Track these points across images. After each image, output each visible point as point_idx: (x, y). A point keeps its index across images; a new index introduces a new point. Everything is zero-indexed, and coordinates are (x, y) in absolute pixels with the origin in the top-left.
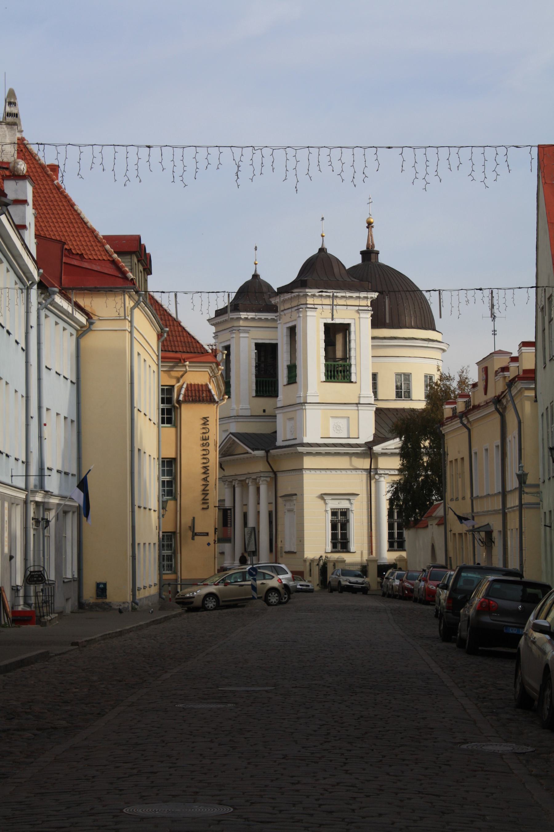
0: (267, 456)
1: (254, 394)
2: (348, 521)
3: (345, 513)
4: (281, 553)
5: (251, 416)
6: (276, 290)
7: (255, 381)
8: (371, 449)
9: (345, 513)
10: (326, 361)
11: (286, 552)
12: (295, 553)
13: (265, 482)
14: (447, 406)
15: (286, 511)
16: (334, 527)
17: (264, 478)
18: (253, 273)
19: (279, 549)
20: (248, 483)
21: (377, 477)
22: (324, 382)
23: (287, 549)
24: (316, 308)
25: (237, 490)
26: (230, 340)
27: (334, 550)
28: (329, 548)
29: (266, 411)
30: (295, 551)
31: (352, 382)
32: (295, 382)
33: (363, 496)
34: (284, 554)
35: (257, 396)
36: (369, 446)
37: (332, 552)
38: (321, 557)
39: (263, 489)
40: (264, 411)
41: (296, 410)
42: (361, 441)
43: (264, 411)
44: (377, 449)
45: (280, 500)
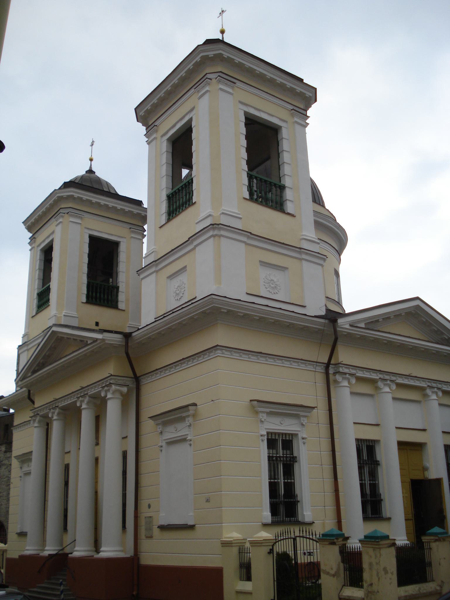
3: (288, 442)
4: (149, 529)
7: (86, 282)
9: (288, 442)
11: (162, 528)
12: (192, 527)
13: (118, 395)
15: (164, 444)
17: (118, 388)
18: (88, 169)
19: (142, 522)
21: (338, 377)
23: (163, 522)
24: (235, 83)
25: (56, 427)
27: (276, 519)
29: (100, 324)
30: (191, 523)
33: (321, 413)
34: (156, 531)
39: (113, 408)
40: (97, 324)
41: (194, 249)
43: (97, 324)
45: (148, 426)
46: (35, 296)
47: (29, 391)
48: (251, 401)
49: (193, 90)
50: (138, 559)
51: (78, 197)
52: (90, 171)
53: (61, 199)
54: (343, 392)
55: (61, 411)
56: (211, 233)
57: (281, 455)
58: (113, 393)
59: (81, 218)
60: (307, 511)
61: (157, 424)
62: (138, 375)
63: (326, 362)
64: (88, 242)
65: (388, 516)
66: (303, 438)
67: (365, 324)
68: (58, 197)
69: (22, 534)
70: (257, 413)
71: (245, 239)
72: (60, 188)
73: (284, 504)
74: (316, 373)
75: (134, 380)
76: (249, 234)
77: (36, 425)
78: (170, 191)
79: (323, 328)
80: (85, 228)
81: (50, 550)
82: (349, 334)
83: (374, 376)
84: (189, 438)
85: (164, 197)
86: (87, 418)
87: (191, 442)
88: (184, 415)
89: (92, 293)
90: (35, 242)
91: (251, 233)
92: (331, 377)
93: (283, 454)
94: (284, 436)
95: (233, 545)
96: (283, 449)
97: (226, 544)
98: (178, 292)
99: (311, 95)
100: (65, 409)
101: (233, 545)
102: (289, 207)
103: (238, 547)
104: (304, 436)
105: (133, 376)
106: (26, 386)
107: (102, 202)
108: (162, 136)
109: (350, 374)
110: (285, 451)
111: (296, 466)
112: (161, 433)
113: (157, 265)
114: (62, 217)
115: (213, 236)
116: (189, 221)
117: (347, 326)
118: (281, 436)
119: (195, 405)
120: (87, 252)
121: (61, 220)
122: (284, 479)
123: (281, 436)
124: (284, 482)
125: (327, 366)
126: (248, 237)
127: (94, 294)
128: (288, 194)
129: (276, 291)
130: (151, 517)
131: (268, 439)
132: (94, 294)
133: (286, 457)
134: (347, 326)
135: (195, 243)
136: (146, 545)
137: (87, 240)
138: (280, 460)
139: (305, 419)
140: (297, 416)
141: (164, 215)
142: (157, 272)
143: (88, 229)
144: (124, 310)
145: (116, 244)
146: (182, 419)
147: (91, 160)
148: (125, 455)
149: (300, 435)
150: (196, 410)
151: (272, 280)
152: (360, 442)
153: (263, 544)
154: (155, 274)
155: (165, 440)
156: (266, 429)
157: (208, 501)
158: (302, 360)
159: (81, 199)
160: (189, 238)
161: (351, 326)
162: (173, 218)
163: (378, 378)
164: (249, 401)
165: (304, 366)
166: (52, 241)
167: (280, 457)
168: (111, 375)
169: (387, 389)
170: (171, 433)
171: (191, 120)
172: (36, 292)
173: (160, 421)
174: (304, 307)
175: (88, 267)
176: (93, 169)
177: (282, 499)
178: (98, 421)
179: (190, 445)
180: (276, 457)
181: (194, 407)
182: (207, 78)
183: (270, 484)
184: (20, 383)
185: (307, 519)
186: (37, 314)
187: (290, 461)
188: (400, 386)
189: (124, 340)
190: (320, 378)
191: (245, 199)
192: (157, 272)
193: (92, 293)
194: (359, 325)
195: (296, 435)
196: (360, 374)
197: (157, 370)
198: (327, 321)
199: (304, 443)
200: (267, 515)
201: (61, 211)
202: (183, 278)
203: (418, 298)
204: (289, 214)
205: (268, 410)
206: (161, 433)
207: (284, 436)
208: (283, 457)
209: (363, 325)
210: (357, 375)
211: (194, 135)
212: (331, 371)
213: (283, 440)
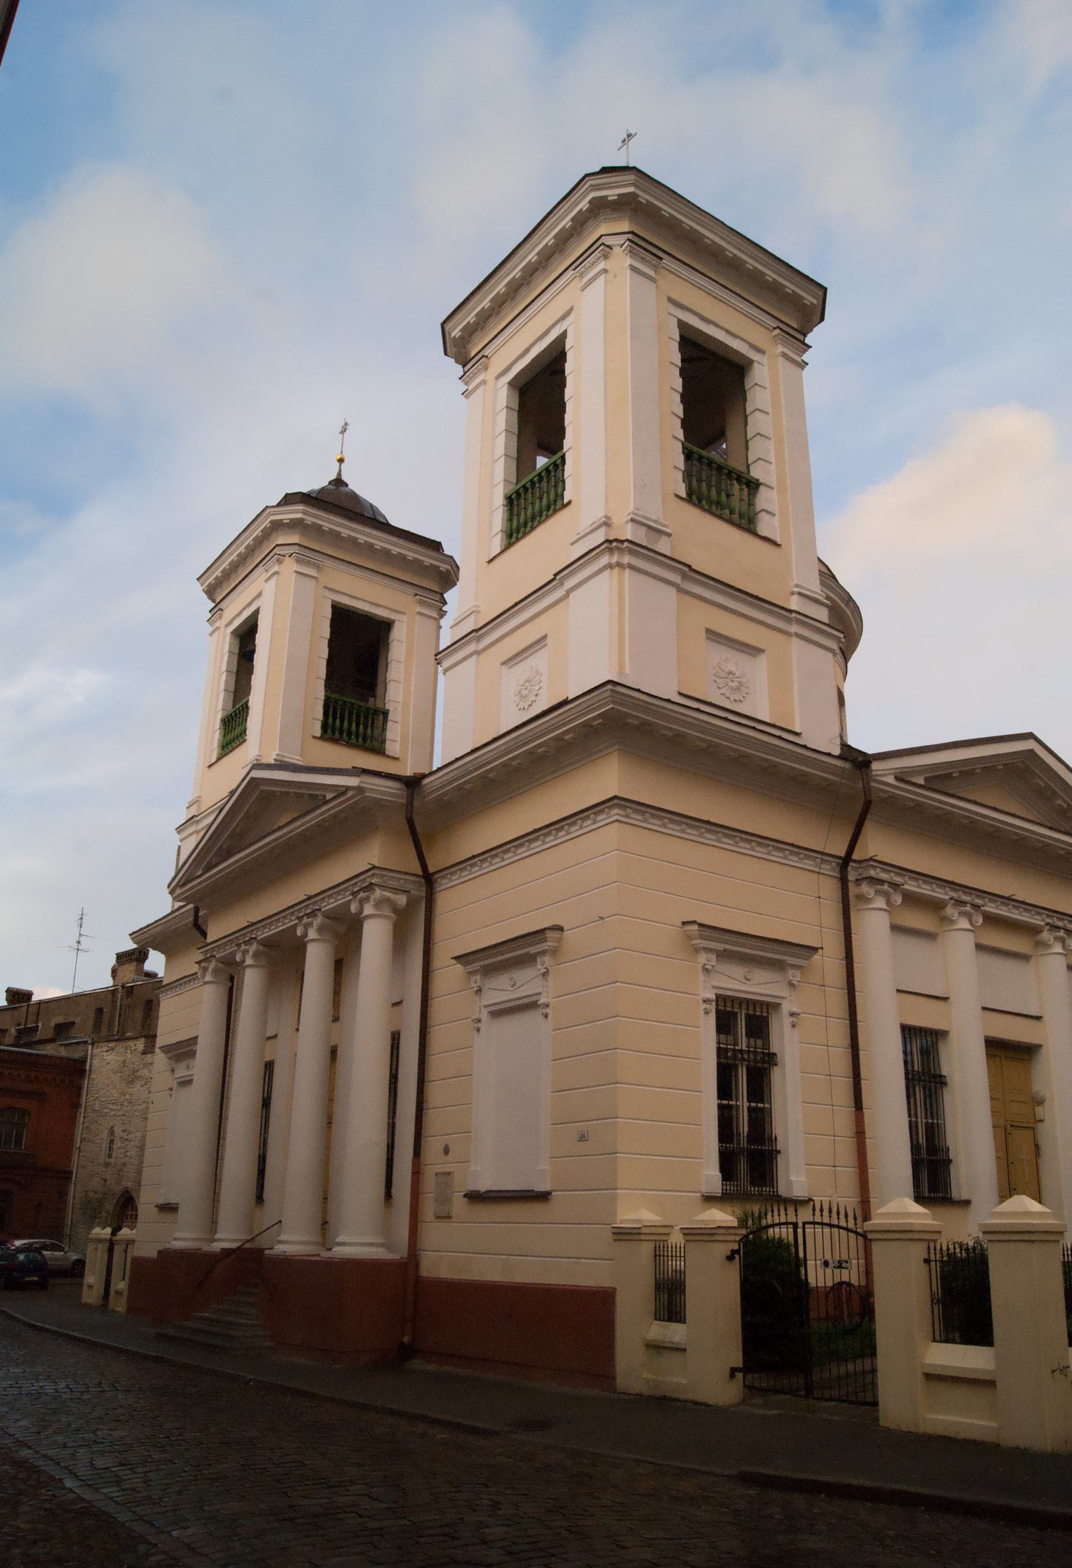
0: (410, 804)
1: (318, 734)
2: (771, 1059)
4: (444, 1199)
11: (475, 1197)
12: (543, 1197)
15: (484, 1015)
17: (387, 894)
18: (334, 477)
19: (429, 1182)
21: (866, 889)
22: (681, 498)
24: (661, 259)
25: (252, 980)
27: (731, 1187)
33: (830, 962)
34: (459, 1205)
35: (322, 738)
39: (376, 935)
45: (449, 976)
46: (218, 724)
47: (197, 910)
48: (684, 923)
49: (570, 273)
50: (417, 1265)
51: (313, 523)
52: (339, 482)
53: (277, 526)
54: (874, 924)
55: (261, 948)
56: (605, 560)
57: (744, 1048)
58: (378, 905)
59: (318, 568)
60: (795, 1176)
61: (471, 973)
62: (431, 870)
63: (842, 854)
64: (330, 616)
65: (965, 1196)
66: (792, 1015)
67: (926, 779)
68: (271, 522)
70: (697, 950)
71: (676, 578)
72: (279, 505)
73: (748, 1156)
74: (821, 877)
75: (423, 881)
76: (687, 569)
77: (208, 978)
78: (512, 488)
79: (839, 780)
80: (325, 587)
81: (227, 1238)
82: (893, 796)
83: (940, 894)
84: (543, 1000)
85: (499, 500)
86: (317, 958)
87: (548, 1011)
88: (532, 950)
89: (334, 719)
90: (220, 617)
91: (689, 567)
92: (853, 889)
94: (751, 1008)
95: (643, 1237)
97: (625, 1235)
98: (525, 692)
99: (815, 302)
100: (269, 944)
101: (643, 1237)
102: (766, 525)
103: (652, 1244)
104: (795, 1009)
106: (188, 900)
107: (362, 538)
108: (497, 378)
110: (752, 1041)
111: (776, 1074)
112: (479, 991)
113: (479, 639)
114: (279, 562)
115: (610, 566)
116: (553, 541)
117: (891, 780)
118: (744, 1007)
119: (561, 929)
120: (328, 635)
121: (276, 568)
123: (744, 1007)
125: (846, 861)
126: (684, 577)
127: (338, 722)
128: (765, 499)
130: (449, 1173)
131: (718, 1011)
132: (338, 722)
133: (755, 1053)
134: (891, 780)
135: (569, 584)
136: (433, 1234)
137: (328, 613)
138: (743, 1059)
139: (797, 973)
140: (778, 966)
141: (499, 536)
142: (477, 653)
143: (331, 590)
144: (397, 759)
145: (383, 628)
146: (528, 960)
147: (341, 461)
148: (395, 1040)
149: (786, 1007)
150: (559, 940)
151: (730, 673)
152: (907, 1031)
153: (716, 1238)
154: (475, 657)
155: (485, 1007)
156: (714, 987)
157: (583, 1138)
158: (792, 845)
159: (318, 528)
160: (555, 575)
161: (897, 778)
162: (518, 540)
163: (947, 897)
164: (680, 924)
165: (796, 859)
166: (256, 613)
167: (742, 1051)
168: (374, 867)
169: (964, 923)
170: (501, 990)
171: (563, 336)
172: (219, 716)
173: (476, 966)
175: (330, 646)
176: (345, 478)
177: (744, 1143)
178: (342, 966)
179: (546, 1016)
180: (734, 1050)
181: (555, 934)
182: (603, 244)
183: (720, 1107)
184: (178, 891)
185: (799, 1191)
186: (219, 759)
187: (763, 1061)
188: (991, 920)
189: (405, 793)
190: (830, 889)
192: (477, 653)
193: (334, 719)
194: (914, 780)
195: (777, 1006)
196: (911, 886)
197: (474, 857)
198: (847, 765)
199: (794, 1026)
200: (710, 1176)
201: (277, 551)
202: (538, 661)
203: (1030, 736)
205: (721, 947)
206: (479, 991)
207: (751, 1008)
208: (748, 1052)
209: (921, 781)
210: (906, 887)
211: (569, 367)
212: (852, 876)
213: (746, 1015)
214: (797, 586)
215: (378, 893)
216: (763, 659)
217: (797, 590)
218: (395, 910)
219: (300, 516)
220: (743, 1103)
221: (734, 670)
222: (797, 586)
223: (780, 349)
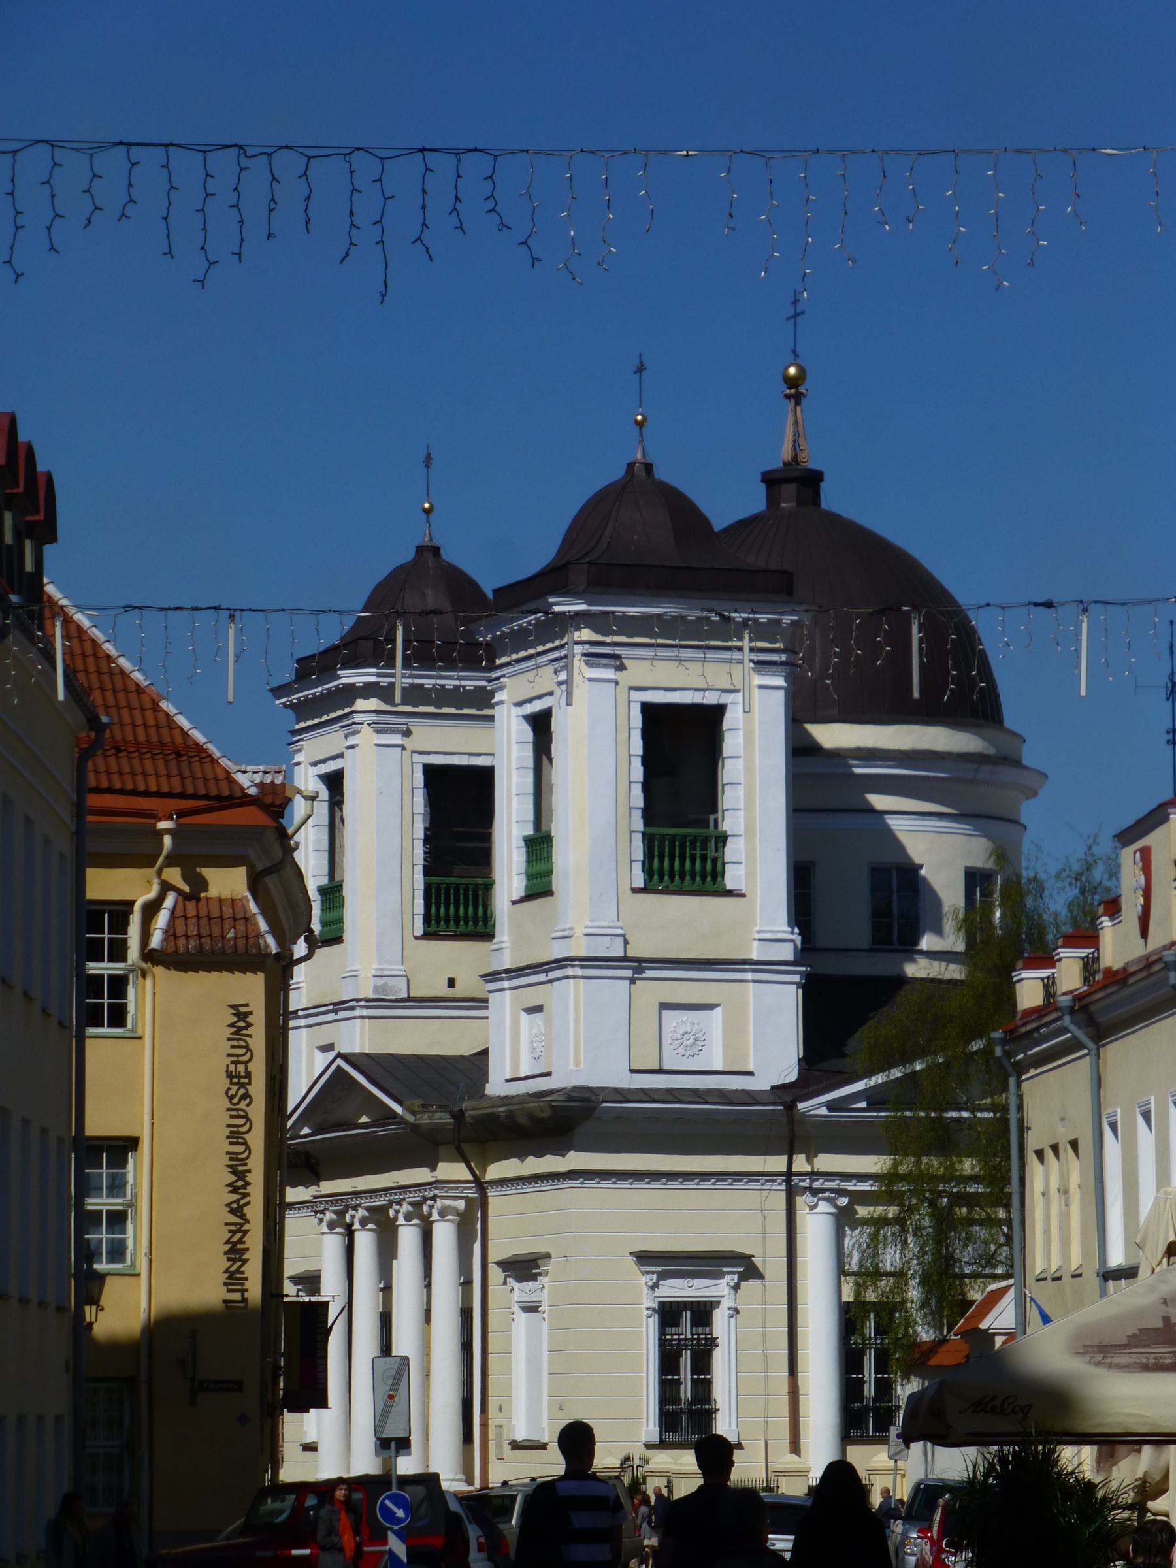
1: (419, 930)
2: (712, 1342)
3: (703, 1312)
4: (499, 1446)
5: (409, 999)
6: (490, 595)
8: (791, 1107)
10: (646, 825)
11: (516, 1446)
14: (1025, 974)
16: (668, 1361)
17: (447, 1202)
20: (396, 1219)
23: (521, 1435)
26: (341, 755)
27: (669, 1437)
28: (650, 1429)
31: (730, 893)
32: (548, 893)
35: (427, 936)
36: (788, 1094)
37: (662, 1445)
38: (627, 1459)
39: (444, 1235)
40: (451, 983)
42: (762, 1083)
43: (451, 983)
44: (815, 1106)
69: (310, 1448)
71: (629, 973)
93: (692, 1334)
96: (692, 1326)
102: (733, 878)
105: (471, 1178)
109: (831, 1190)
117: (824, 1111)
119: (547, 1256)
122: (692, 1374)
124: (692, 1380)
128: (733, 851)
129: (700, 1043)
133: (699, 1339)
134: (824, 1111)
138: (686, 1345)
157: (561, 1408)
167: (686, 1339)
174: (751, 1074)
180: (679, 1340)
187: (706, 1345)
191: (635, 890)
204: (730, 893)
208: (692, 1339)
214: (759, 932)
215: (439, 1202)
216: (719, 1010)
217: (757, 936)
218: (458, 1214)
219: (373, 679)
220: (686, 1374)
221: (688, 1029)
222: (759, 932)
223: (758, 680)
